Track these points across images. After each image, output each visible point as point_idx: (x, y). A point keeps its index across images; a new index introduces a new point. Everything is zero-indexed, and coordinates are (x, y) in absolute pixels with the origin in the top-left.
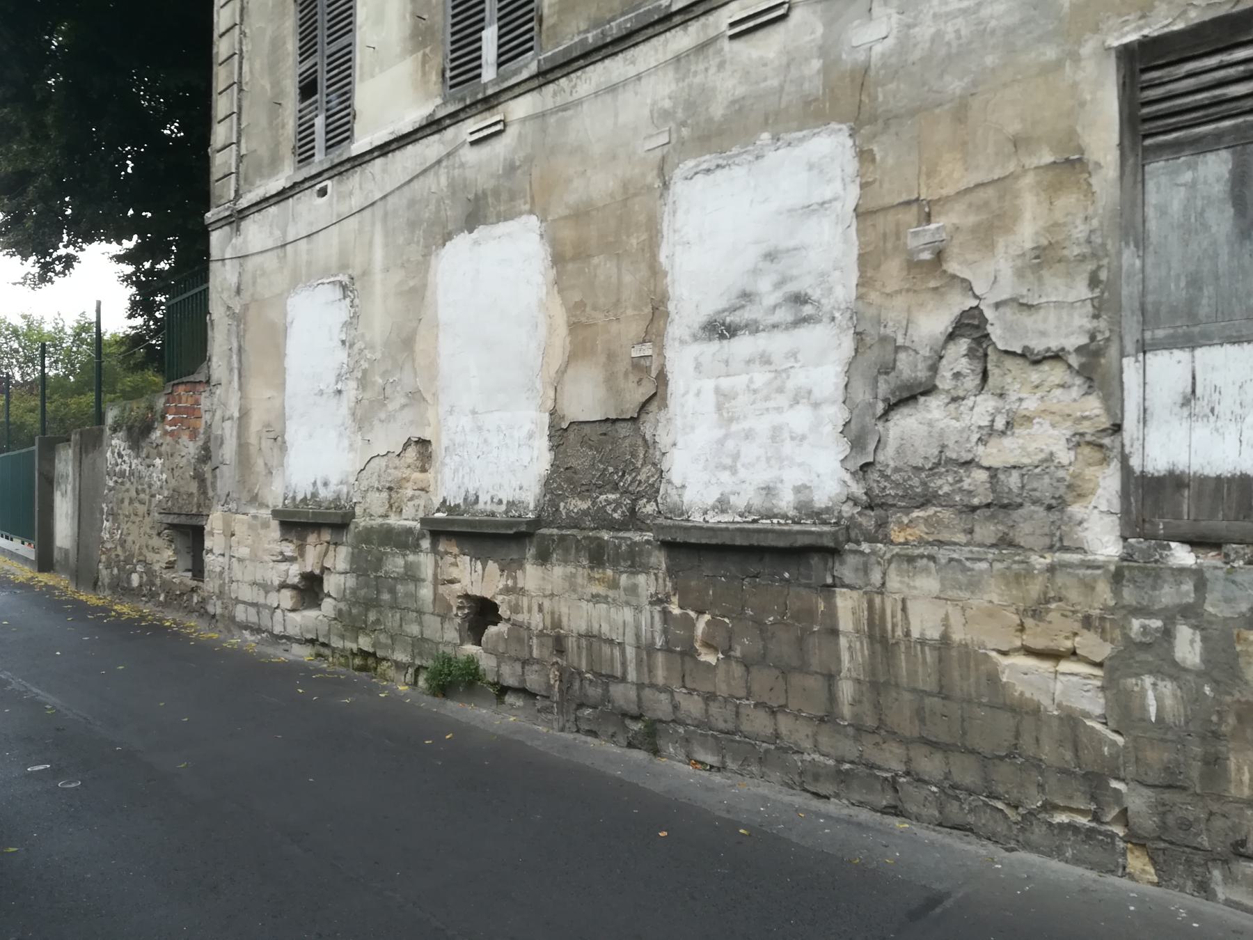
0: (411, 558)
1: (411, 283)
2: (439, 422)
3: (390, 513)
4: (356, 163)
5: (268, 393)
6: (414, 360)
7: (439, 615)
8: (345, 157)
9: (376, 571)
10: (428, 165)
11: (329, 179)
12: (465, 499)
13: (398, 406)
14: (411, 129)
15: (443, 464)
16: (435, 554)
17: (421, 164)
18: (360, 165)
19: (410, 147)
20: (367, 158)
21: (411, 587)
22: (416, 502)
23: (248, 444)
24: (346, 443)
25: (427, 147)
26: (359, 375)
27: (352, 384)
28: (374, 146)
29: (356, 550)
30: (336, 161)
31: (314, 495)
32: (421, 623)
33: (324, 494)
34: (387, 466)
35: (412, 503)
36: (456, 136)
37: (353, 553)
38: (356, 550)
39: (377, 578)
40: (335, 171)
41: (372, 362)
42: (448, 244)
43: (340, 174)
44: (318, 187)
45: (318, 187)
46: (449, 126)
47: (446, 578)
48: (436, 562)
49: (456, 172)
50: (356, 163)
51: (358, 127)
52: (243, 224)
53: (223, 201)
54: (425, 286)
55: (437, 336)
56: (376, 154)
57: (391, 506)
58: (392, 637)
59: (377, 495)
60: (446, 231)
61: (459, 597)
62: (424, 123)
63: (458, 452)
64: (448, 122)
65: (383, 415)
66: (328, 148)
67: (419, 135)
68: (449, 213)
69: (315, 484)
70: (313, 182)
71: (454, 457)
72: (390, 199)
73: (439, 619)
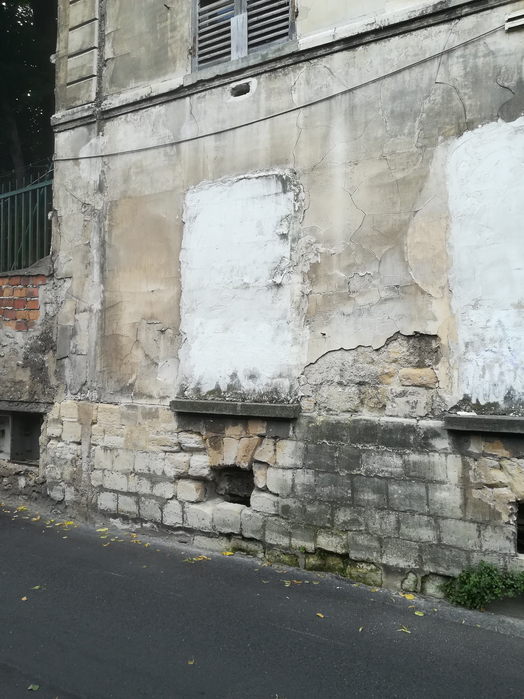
0: (414, 457)
1: (399, 176)
2: (453, 316)
3: (361, 409)
4: (303, 58)
5: (147, 287)
6: (402, 253)
7: (472, 521)
8: (287, 51)
9: (349, 468)
10: (427, 56)
11: (252, 76)
12: (508, 398)
13: (375, 300)
14: (406, 19)
15: (462, 359)
16: (463, 455)
17: (416, 55)
18: (308, 60)
19: (397, 38)
20: (322, 52)
21: (419, 489)
22: (412, 399)
23: (116, 337)
24: (289, 336)
25: (426, 37)
26: (306, 269)
27: (297, 278)
28: (337, 38)
29: (312, 446)
30: (271, 56)
31: (230, 388)
32: (437, 528)
33: (247, 385)
34: (355, 361)
35: (404, 399)
36: (477, 26)
37: (306, 449)
38: (312, 446)
39: (351, 477)
40: (266, 68)
41: (328, 257)
42: (467, 135)
43: (274, 70)
44: (233, 85)
45: (233, 85)
46: (467, 15)
47: (485, 481)
48: (466, 466)
49: (480, 61)
50: (303, 58)
51: (300, 24)
52: (108, 125)
53: (78, 103)
54: (425, 177)
55: (447, 228)
56: (336, 48)
57: (362, 402)
58: (380, 539)
59: (340, 389)
60: (463, 120)
61: (510, 503)
62: (430, 11)
63: (490, 347)
64: (466, 10)
65: (348, 309)
66: (250, 46)
67: (413, 26)
68: (467, 103)
69: (234, 376)
70: (227, 80)
71: (483, 353)
72: (358, 92)
73: (474, 526)
